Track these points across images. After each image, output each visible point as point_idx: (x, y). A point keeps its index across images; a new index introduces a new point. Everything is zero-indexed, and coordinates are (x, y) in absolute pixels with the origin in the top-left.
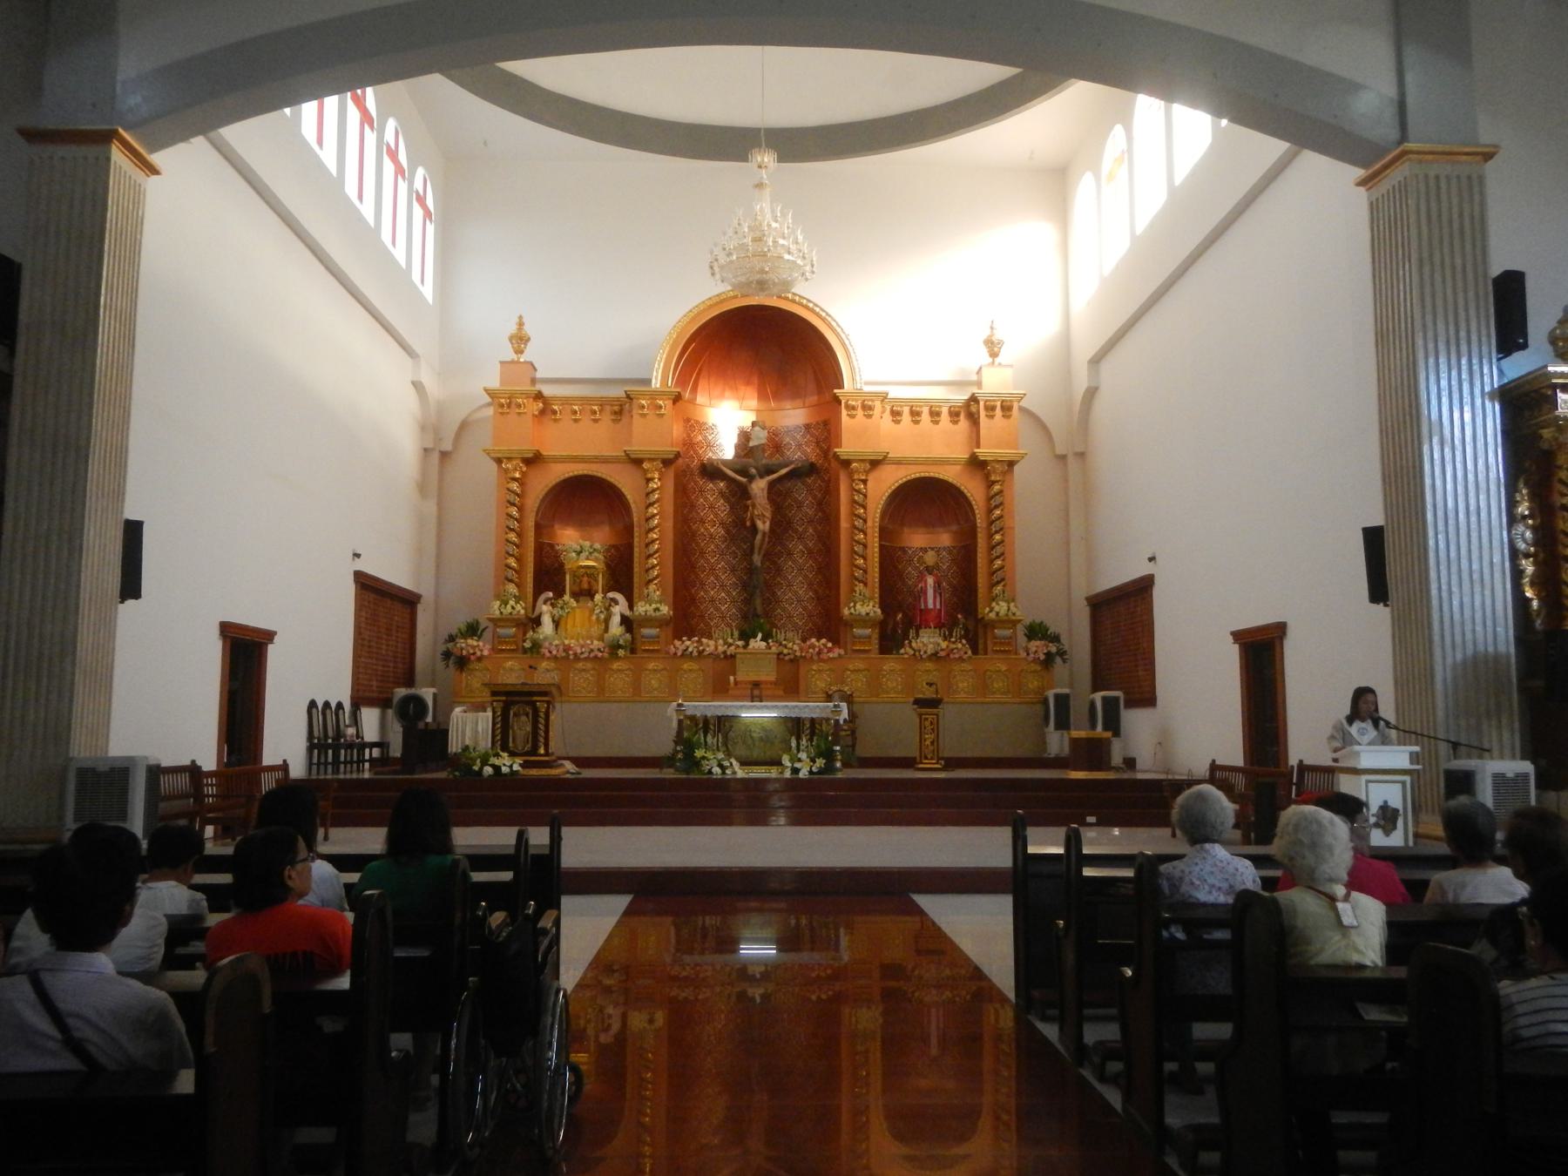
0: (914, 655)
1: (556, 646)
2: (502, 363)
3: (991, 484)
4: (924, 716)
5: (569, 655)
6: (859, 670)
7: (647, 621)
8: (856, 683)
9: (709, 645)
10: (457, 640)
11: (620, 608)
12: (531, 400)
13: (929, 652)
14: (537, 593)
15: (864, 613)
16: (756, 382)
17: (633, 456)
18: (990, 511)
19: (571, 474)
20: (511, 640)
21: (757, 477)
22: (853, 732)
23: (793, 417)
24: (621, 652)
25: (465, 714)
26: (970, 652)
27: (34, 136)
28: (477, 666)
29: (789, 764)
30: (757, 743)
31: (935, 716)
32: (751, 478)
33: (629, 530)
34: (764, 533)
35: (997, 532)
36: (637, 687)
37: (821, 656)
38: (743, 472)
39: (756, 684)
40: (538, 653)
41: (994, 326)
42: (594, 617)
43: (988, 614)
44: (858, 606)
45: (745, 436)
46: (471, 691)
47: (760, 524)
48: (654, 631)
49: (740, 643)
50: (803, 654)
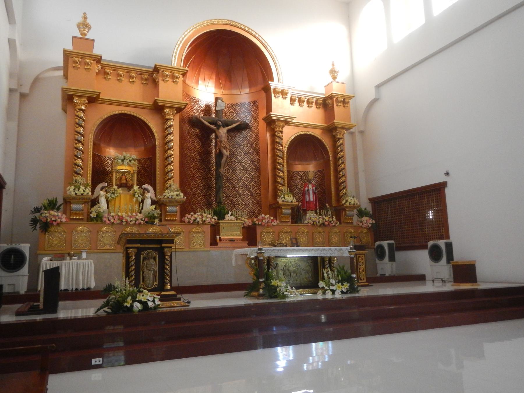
0: (313, 224)
1: (113, 216)
2: (74, 37)
3: (340, 139)
4: (358, 255)
5: (122, 221)
6: (287, 232)
7: (172, 202)
10: (42, 211)
12: (95, 62)
13: (321, 222)
15: (290, 201)
16: (214, 78)
17: (160, 104)
18: (335, 153)
19: (117, 112)
20: (80, 212)
21: (222, 127)
25: (52, 262)
26: (338, 223)
28: (60, 229)
29: (327, 288)
30: (292, 274)
31: (363, 255)
32: (218, 127)
34: (227, 157)
35: (342, 163)
37: (269, 224)
40: (101, 220)
41: (335, 63)
42: (135, 199)
43: (345, 203)
44: (286, 197)
46: (51, 246)
50: (260, 223)
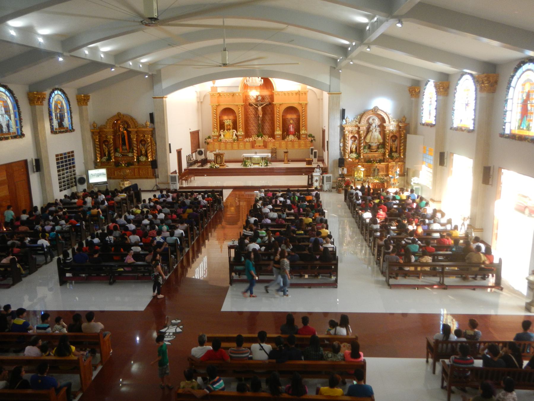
3: (303, 107)
7: (240, 136)
8: (277, 146)
9: (251, 139)
11: (235, 132)
14: (220, 129)
22: (276, 155)
23: (266, 93)
24: (235, 141)
27: (154, 98)
32: (258, 106)
33: (236, 116)
36: (238, 147)
38: (256, 105)
39: (260, 146)
45: (257, 97)
47: (260, 116)
48: (241, 137)
49: (257, 138)
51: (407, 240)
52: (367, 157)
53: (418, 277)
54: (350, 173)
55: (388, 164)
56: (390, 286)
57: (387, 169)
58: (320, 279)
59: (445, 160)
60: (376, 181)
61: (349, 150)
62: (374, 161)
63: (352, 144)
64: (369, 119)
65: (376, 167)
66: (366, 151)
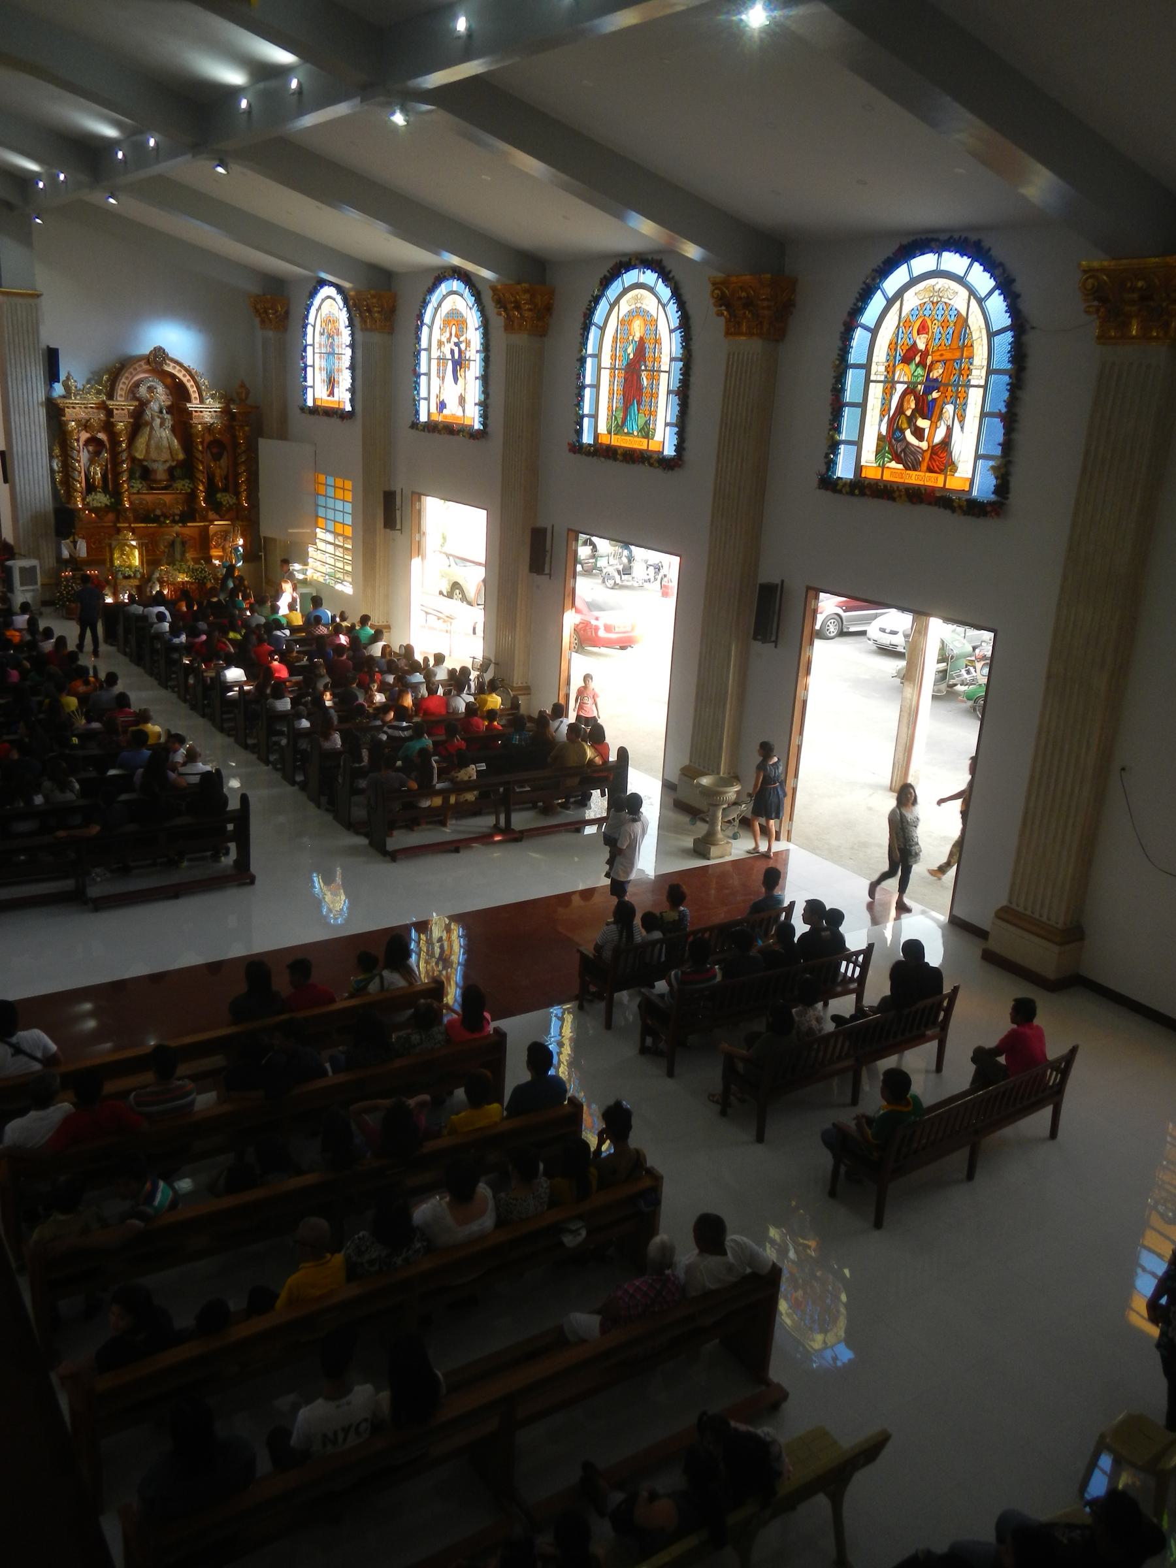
51: (390, 731)
52: (141, 503)
53: (443, 823)
54: (101, 553)
55: (206, 528)
56: (393, 856)
57: (204, 542)
58: (186, 871)
59: (398, 513)
60: (182, 578)
61: (83, 484)
62: (166, 517)
63: (92, 461)
64: (137, 385)
65: (178, 535)
66: (138, 485)
